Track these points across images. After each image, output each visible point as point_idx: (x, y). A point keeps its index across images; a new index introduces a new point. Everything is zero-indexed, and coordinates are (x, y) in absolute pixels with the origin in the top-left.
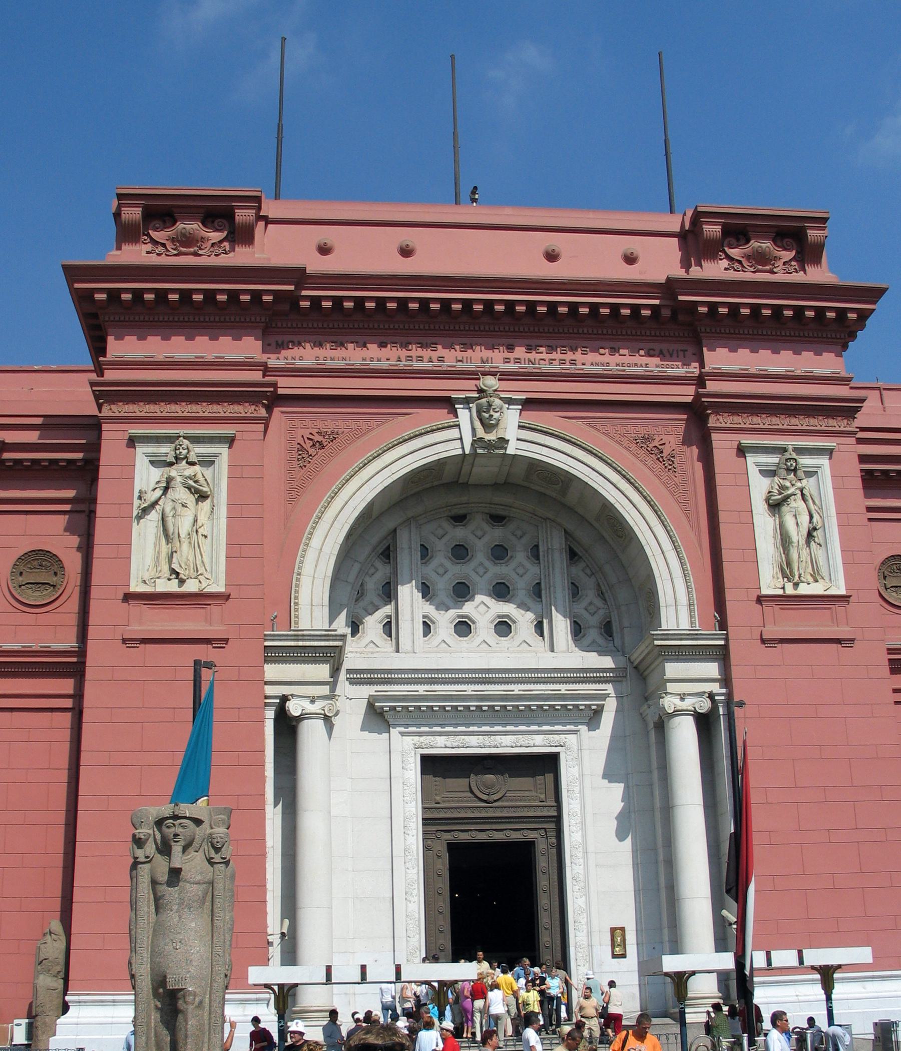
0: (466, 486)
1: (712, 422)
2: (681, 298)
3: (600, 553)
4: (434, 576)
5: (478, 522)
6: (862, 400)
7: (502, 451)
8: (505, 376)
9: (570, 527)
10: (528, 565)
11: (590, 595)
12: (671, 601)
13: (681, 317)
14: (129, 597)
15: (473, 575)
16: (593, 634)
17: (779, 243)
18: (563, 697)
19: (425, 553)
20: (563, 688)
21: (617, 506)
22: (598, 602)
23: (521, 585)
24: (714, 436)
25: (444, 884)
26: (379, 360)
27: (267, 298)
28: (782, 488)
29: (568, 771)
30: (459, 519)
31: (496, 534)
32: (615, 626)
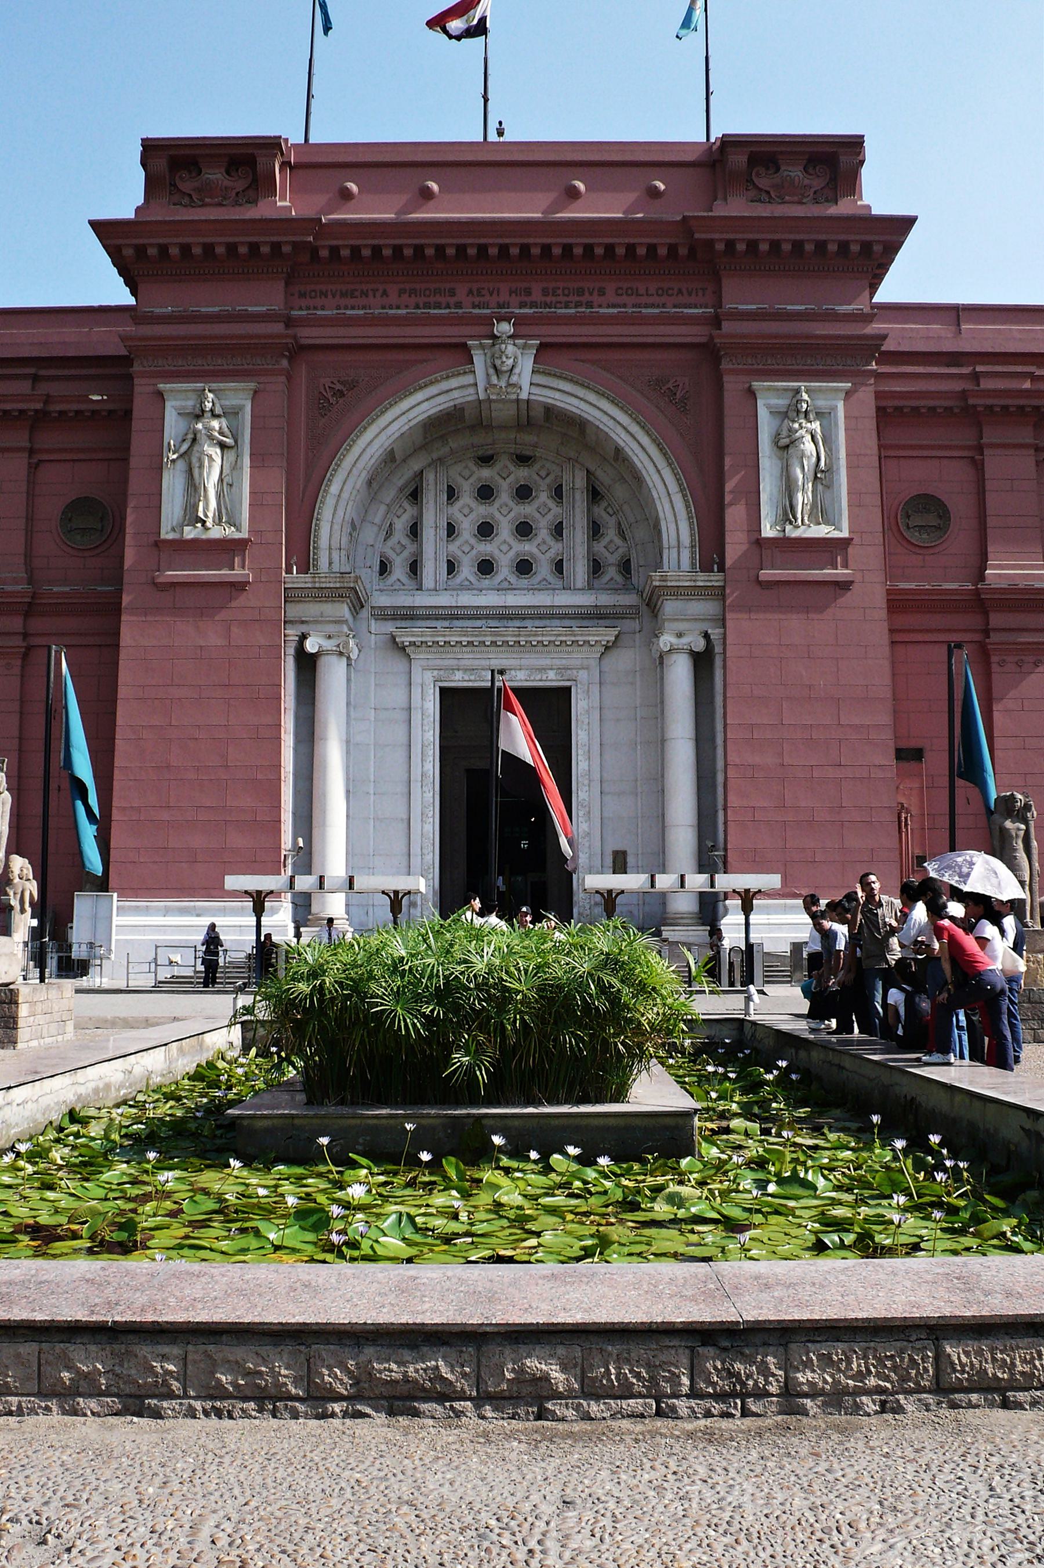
0: (489, 427)
1: (725, 365)
2: (697, 236)
3: (620, 492)
4: (459, 516)
5: (504, 462)
6: (884, 337)
7: (514, 397)
9: (592, 468)
10: (551, 504)
12: (673, 543)
15: (497, 515)
16: (612, 573)
17: (811, 170)
19: (452, 494)
21: (627, 449)
22: (618, 541)
24: (726, 378)
26: (398, 307)
28: (791, 430)
30: (486, 460)
31: (522, 474)
32: (633, 565)
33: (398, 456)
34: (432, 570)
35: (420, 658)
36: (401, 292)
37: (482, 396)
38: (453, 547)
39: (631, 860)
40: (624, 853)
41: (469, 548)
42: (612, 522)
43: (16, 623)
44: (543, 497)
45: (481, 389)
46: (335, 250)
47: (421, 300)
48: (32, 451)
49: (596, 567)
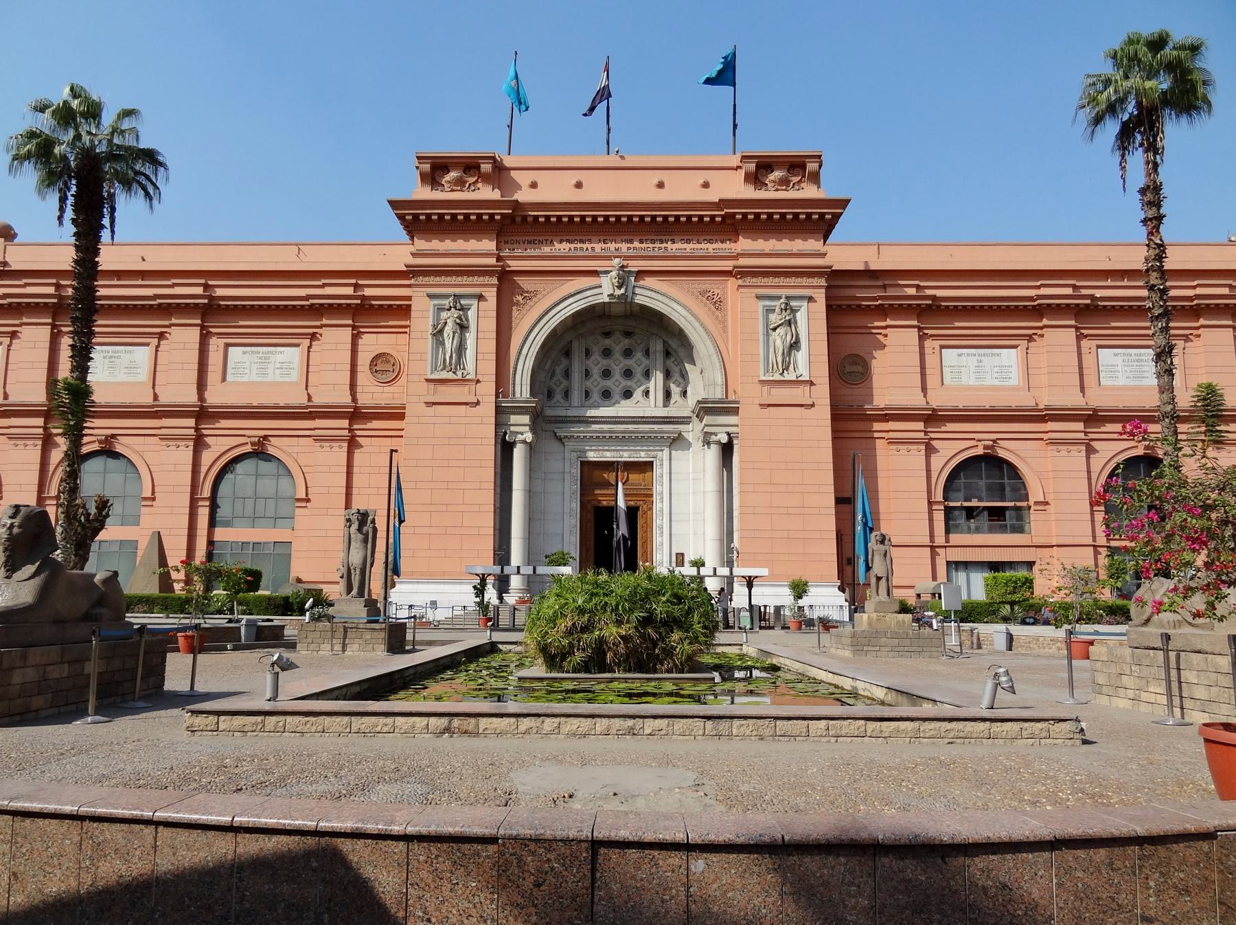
0: (609, 317)
3: (682, 353)
5: (617, 335)
8: (627, 258)
10: (643, 359)
11: (676, 376)
13: (728, 221)
14: (427, 380)
18: (655, 432)
20: (656, 427)
22: (681, 380)
23: (638, 372)
25: (591, 525)
27: (498, 217)
29: (657, 470)
30: (607, 334)
31: (626, 342)
33: (559, 333)
34: (576, 396)
35: (570, 445)
36: (561, 242)
37: (607, 300)
38: (588, 383)
39: (687, 559)
40: (682, 555)
41: (597, 383)
42: (676, 369)
43: (345, 423)
44: (639, 355)
45: (605, 295)
46: (525, 218)
47: (572, 246)
48: (354, 327)
49: (668, 395)
